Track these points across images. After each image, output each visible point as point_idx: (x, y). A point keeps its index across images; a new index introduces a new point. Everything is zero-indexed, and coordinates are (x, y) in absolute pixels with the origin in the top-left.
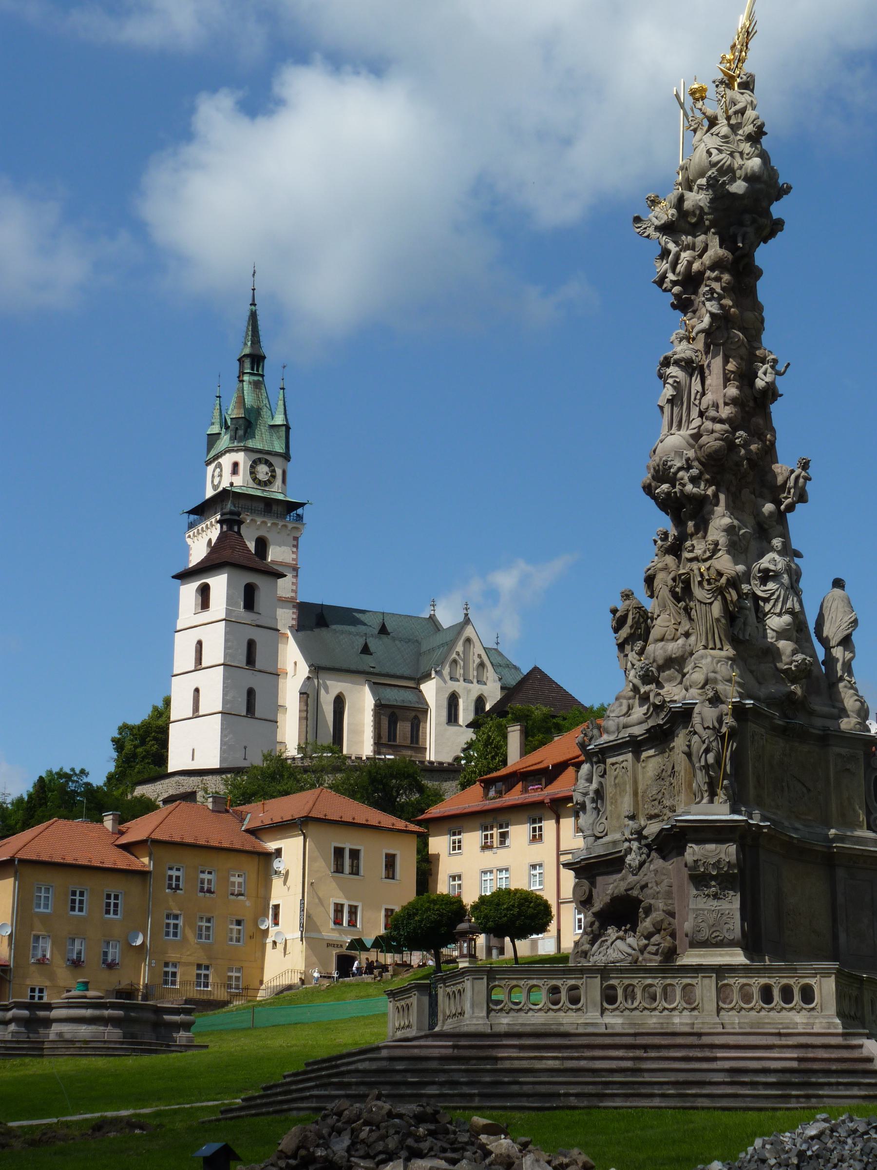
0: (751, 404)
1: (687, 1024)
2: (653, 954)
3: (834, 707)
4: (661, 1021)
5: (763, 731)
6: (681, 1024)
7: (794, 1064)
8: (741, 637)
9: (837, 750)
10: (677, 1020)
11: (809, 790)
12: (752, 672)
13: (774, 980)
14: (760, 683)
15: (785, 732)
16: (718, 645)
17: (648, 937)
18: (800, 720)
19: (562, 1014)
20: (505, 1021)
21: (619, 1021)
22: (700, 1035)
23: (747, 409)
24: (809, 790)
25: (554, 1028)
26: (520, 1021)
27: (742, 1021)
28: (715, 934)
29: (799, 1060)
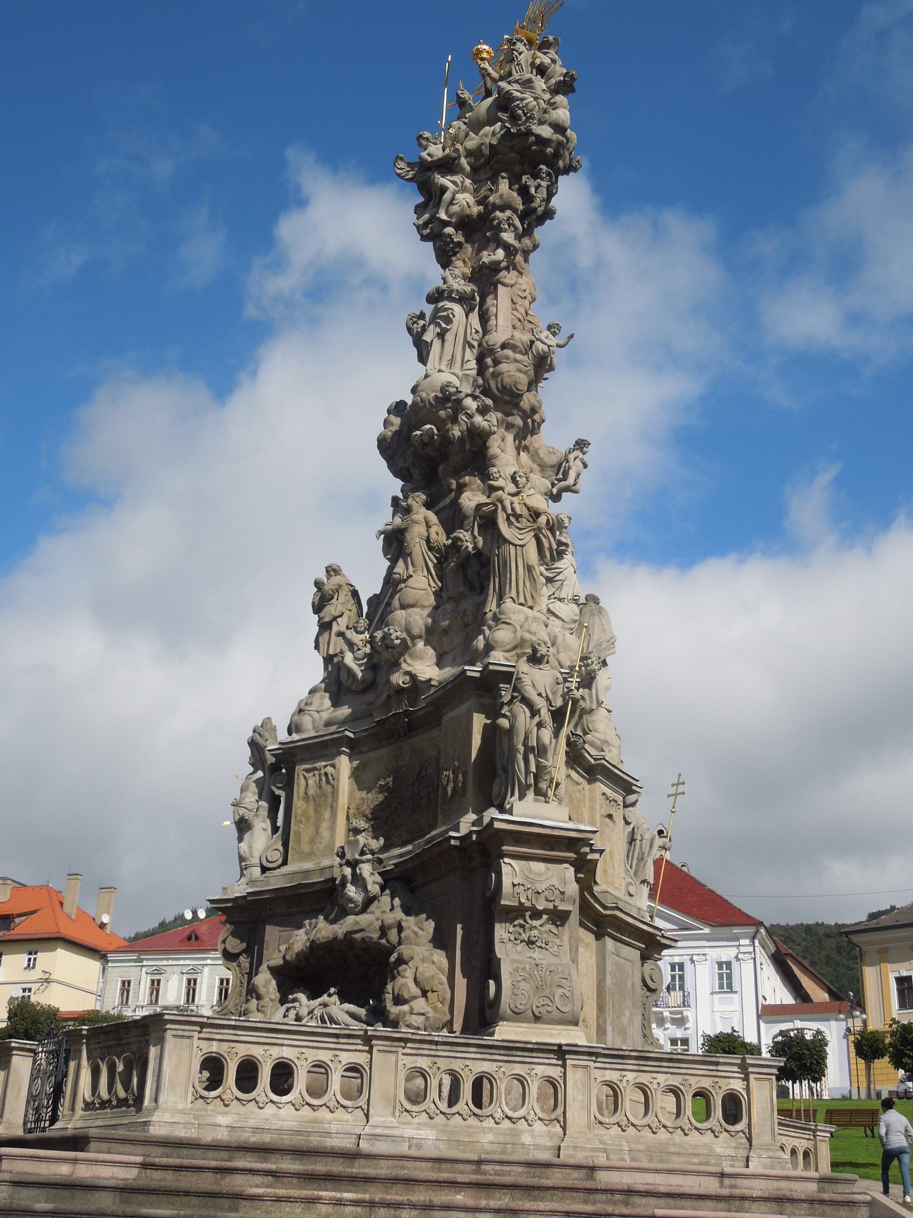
1: (547, 1148)
4: (501, 1139)
6: (537, 1147)
10: (527, 1139)
20: (223, 1120)
22: (592, 1169)
25: (315, 1141)
26: (252, 1122)
27: (634, 1146)
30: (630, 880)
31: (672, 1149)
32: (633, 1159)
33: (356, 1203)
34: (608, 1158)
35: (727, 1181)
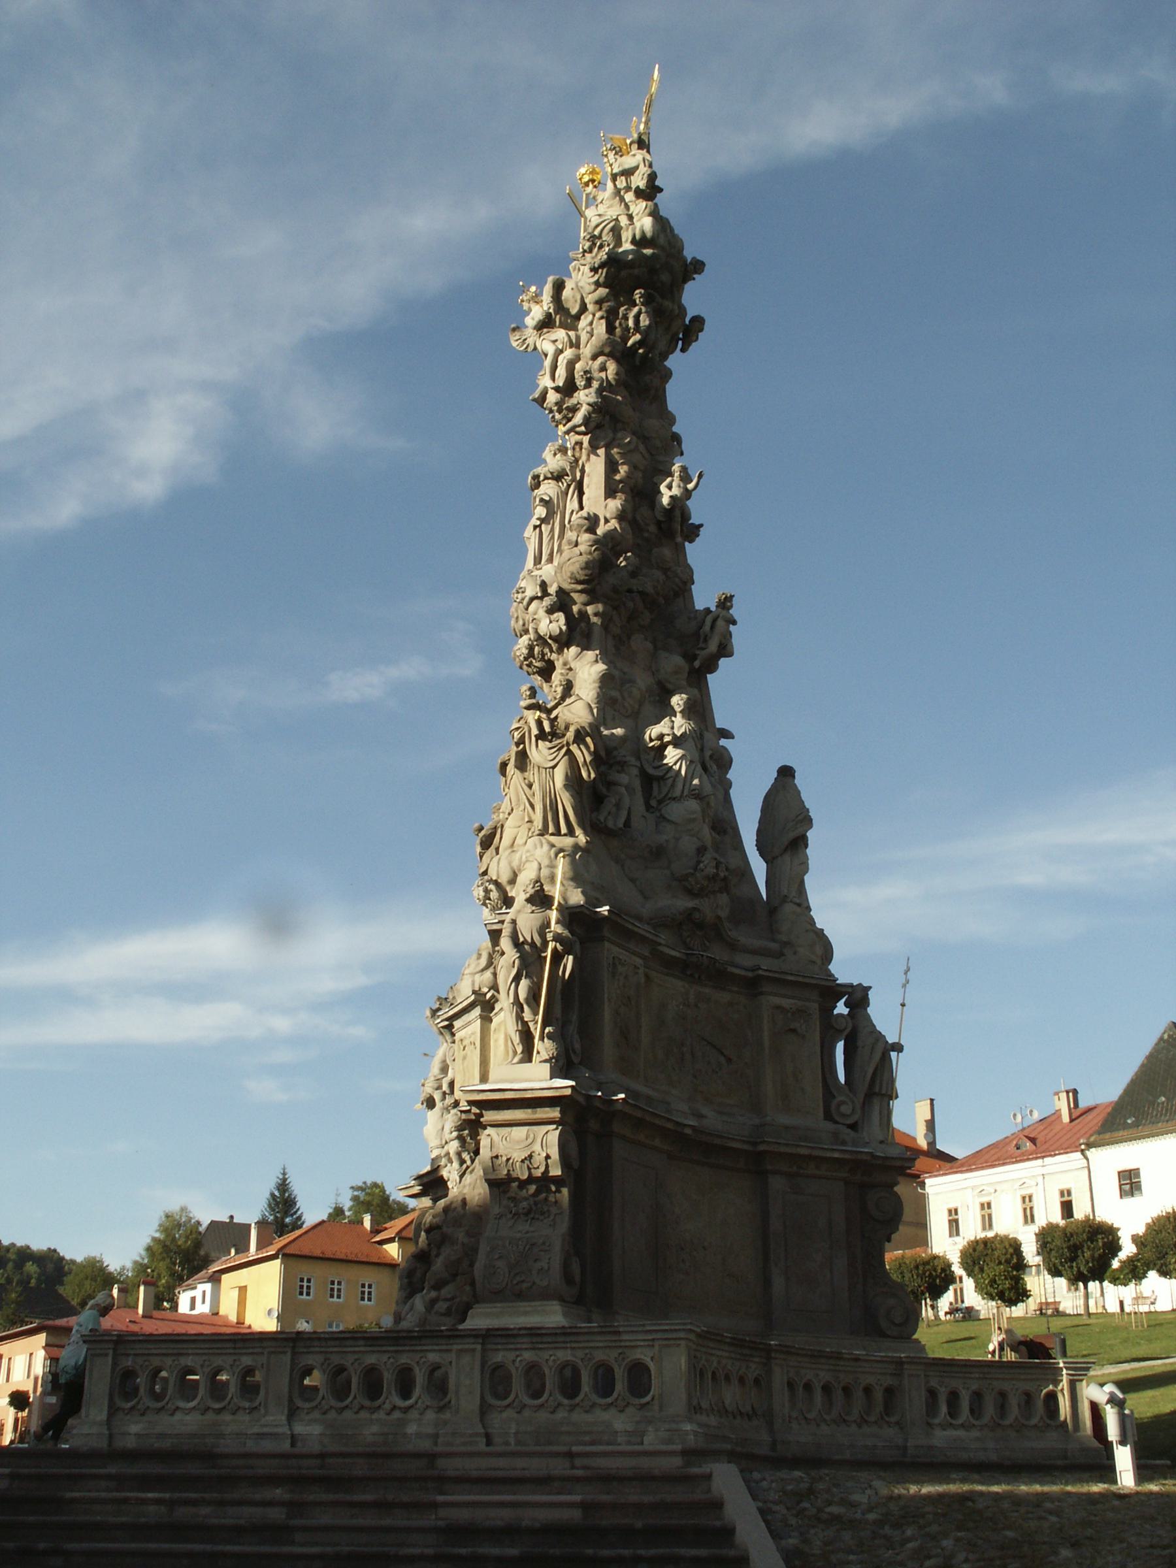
0: (653, 528)
2: (442, 1315)
3: (773, 940)
5: (639, 961)
7: (576, 1515)
8: (610, 824)
9: (777, 1001)
11: (729, 1060)
12: (633, 880)
13: (580, 1354)
14: (646, 898)
15: (684, 968)
16: (564, 830)
17: (437, 1287)
18: (718, 953)
19: (227, 1417)
20: (134, 1429)
21: (316, 1429)
22: (432, 1457)
23: (646, 535)
24: (729, 1060)
28: (518, 1279)
29: (585, 1506)
30: (843, 1098)
31: (564, 1429)
32: (518, 1443)
33: (158, 1502)
34: (489, 1443)
35: (578, 1462)
